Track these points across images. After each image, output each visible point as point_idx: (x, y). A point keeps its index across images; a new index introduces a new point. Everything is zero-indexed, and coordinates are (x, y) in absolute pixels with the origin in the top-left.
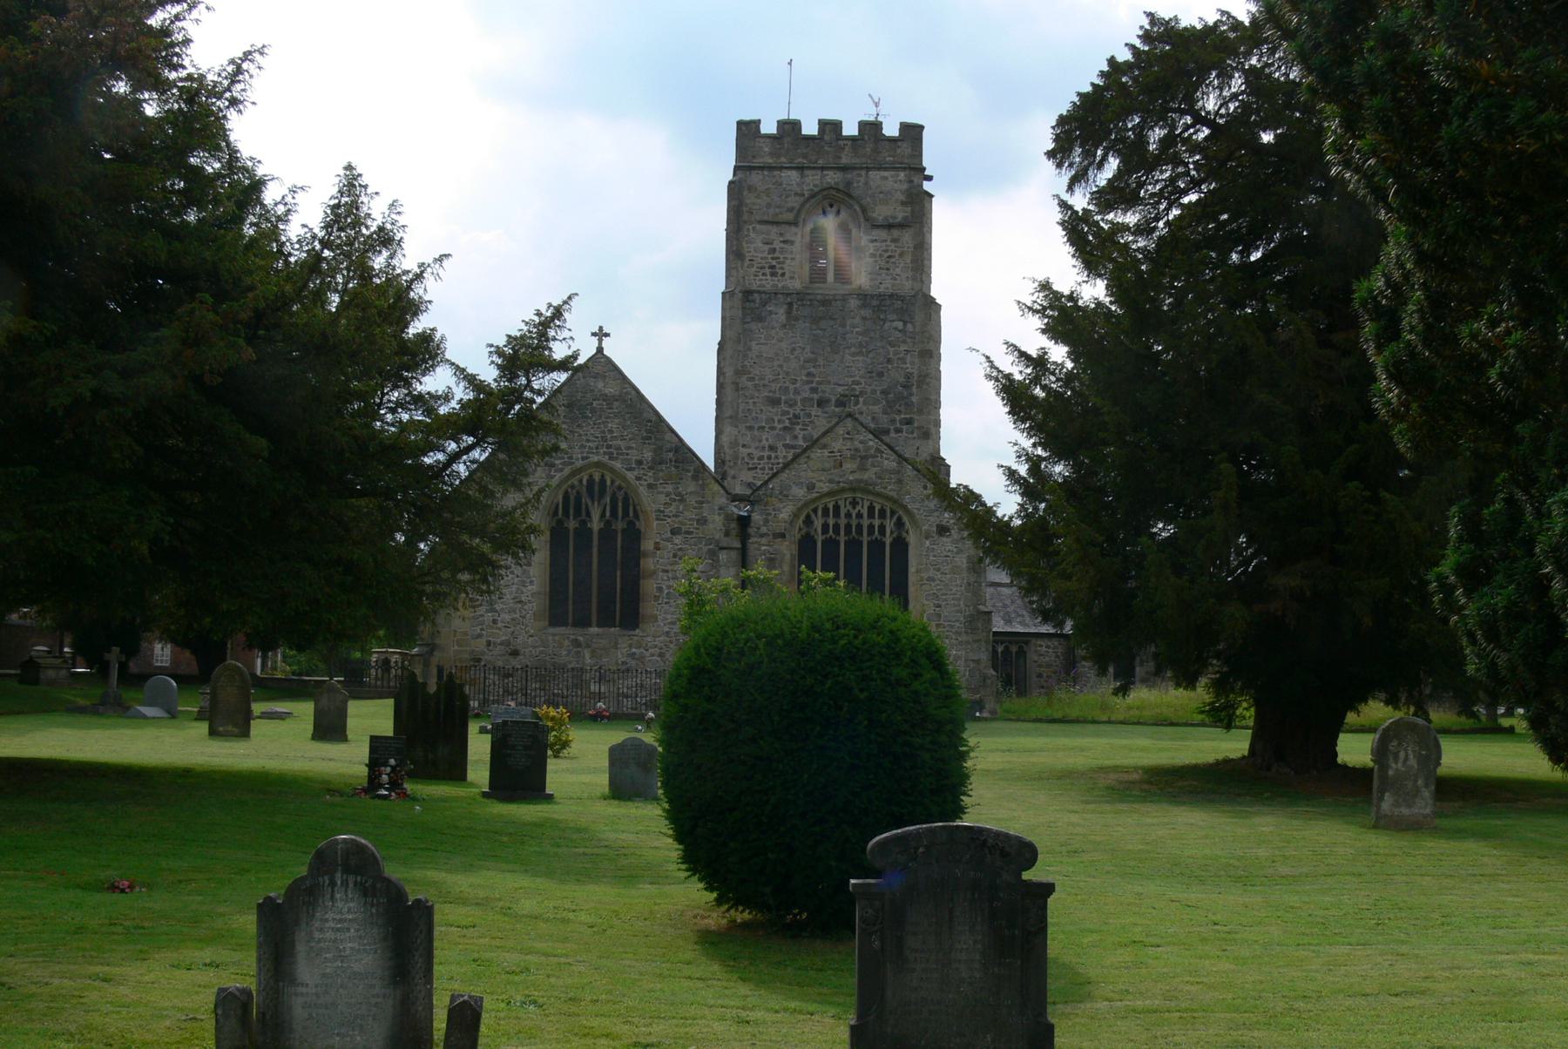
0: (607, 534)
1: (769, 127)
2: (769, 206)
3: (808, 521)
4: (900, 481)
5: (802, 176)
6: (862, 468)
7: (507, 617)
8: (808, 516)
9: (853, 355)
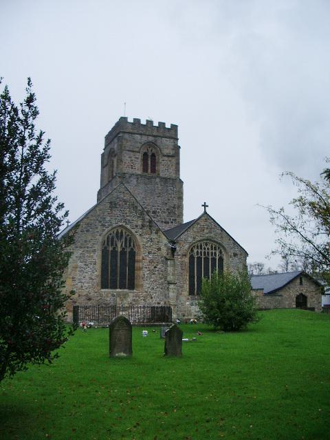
0: (123, 253)
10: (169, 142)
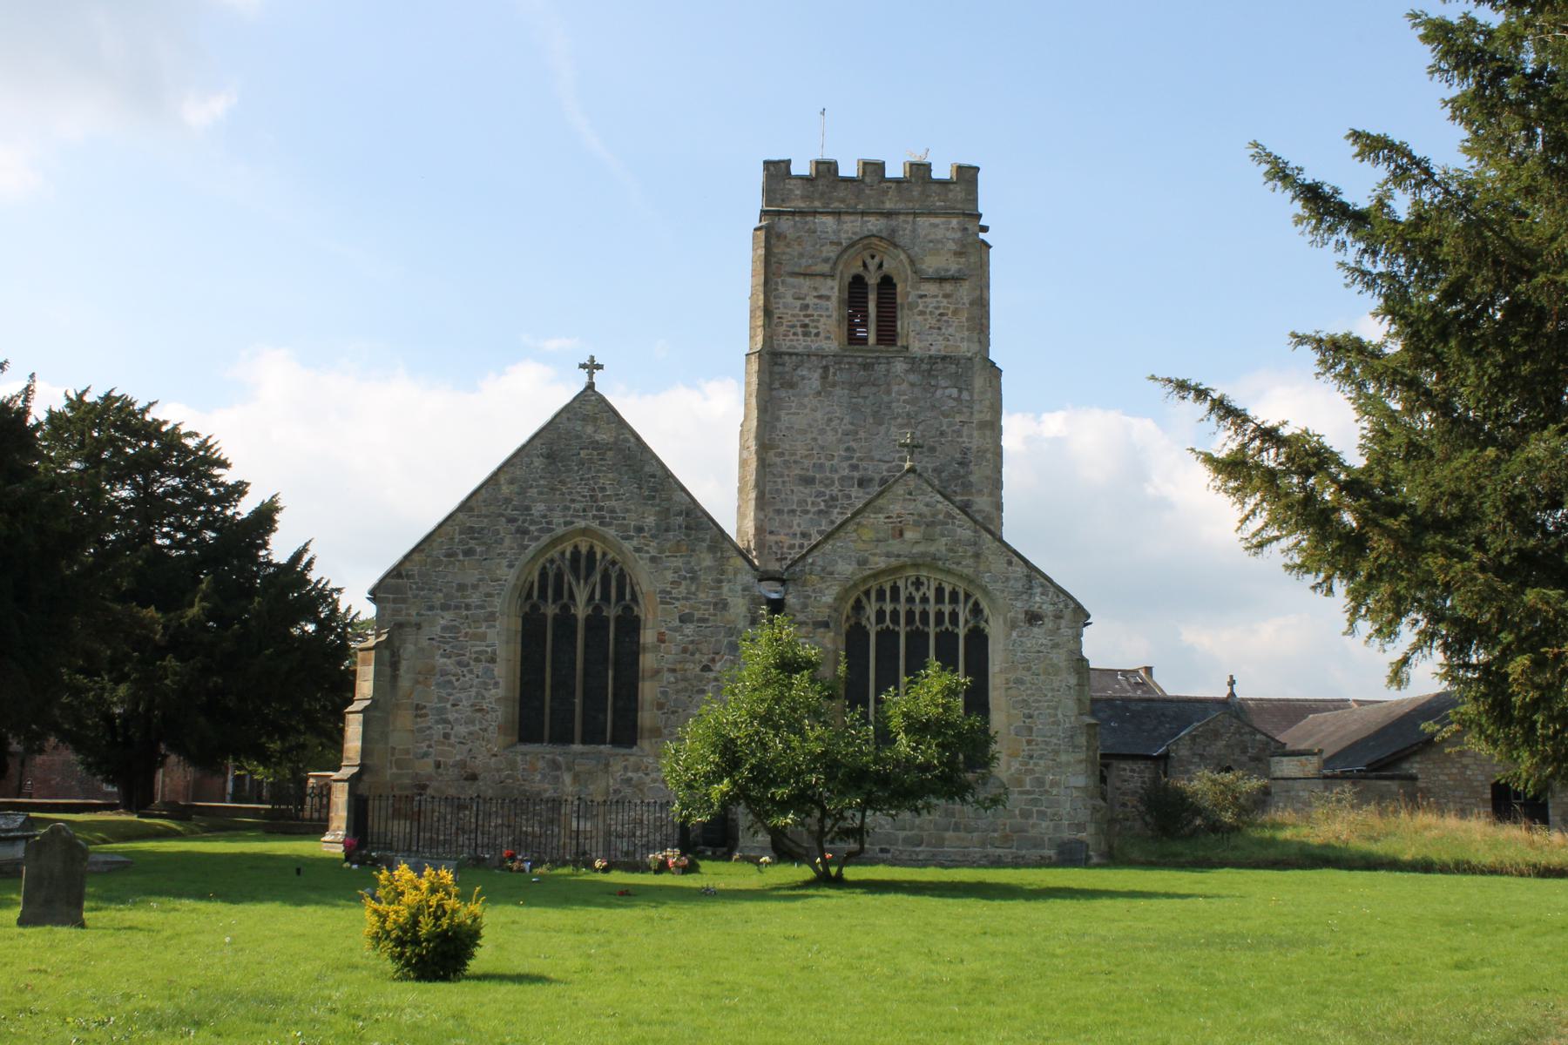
0: (596, 623)
1: (801, 168)
2: (801, 255)
3: (858, 607)
4: (977, 556)
5: (839, 222)
6: (929, 539)
7: (462, 730)
8: (858, 601)
9: (901, 426)
10: (946, 230)
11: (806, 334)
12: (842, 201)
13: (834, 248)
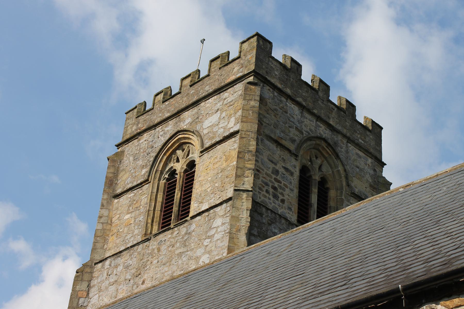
11: (275, 196)
12: (305, 100)
13: (297, 133)
